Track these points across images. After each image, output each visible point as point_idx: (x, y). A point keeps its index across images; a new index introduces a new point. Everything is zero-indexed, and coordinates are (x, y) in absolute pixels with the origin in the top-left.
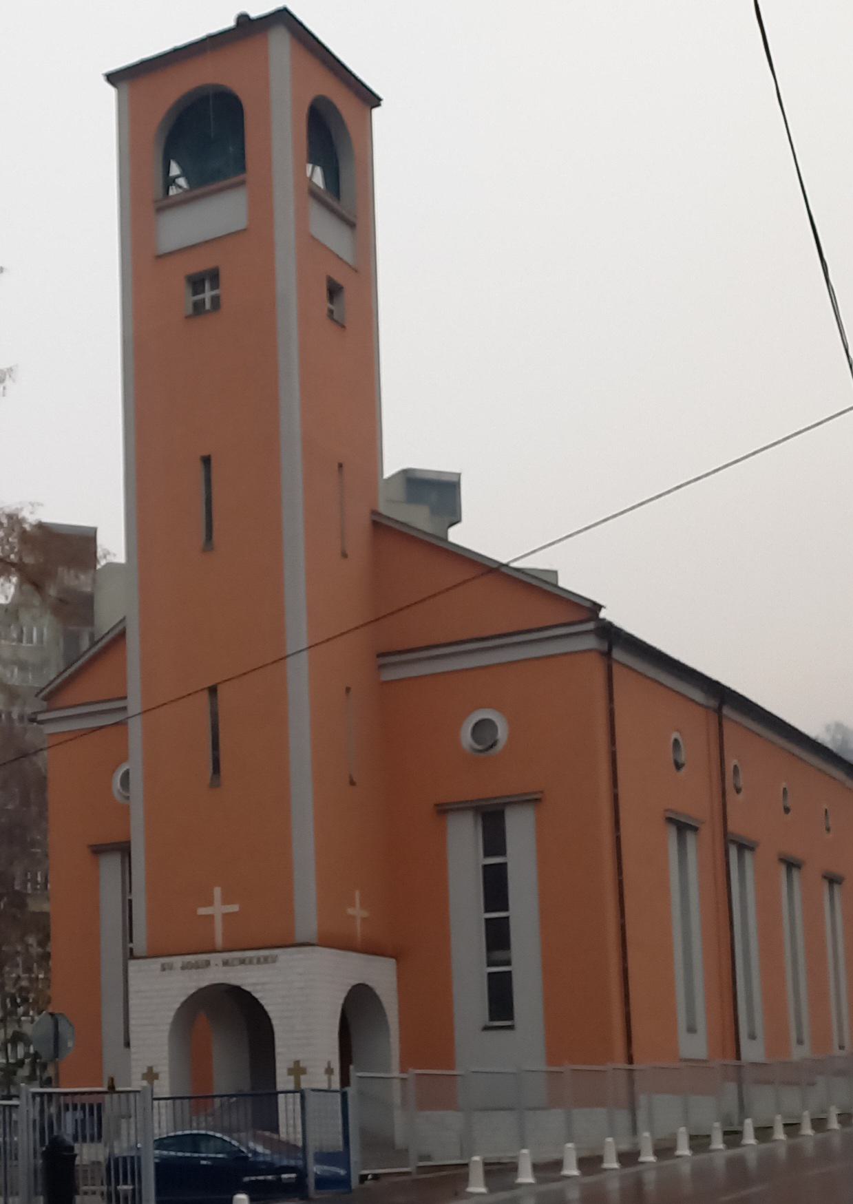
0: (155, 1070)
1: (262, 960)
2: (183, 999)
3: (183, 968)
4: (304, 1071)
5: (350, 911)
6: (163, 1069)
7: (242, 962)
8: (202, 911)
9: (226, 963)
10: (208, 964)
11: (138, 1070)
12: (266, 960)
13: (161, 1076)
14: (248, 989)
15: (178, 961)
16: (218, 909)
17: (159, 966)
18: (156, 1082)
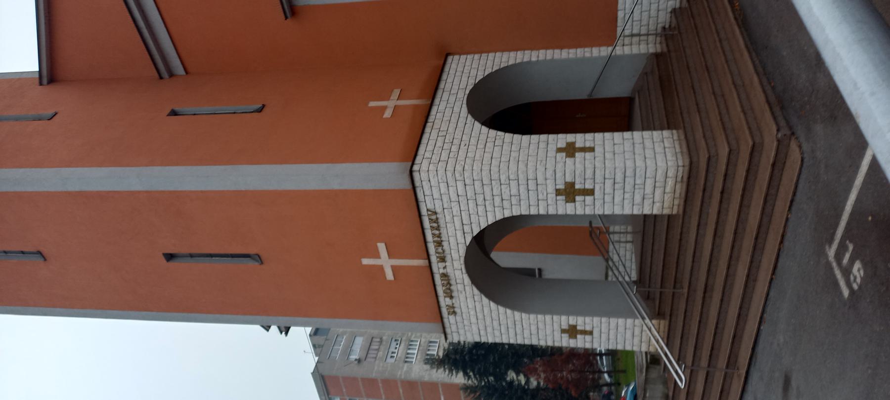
0: (565, 326)
1: (435, 225)
2: (485, 300)
3: (451, 297)
5: (388, 114)
6: (565, 321)
7: (439, 244)
8: (390, 276)
9: (443, 259)
10: (445, 276)
11: (566, 342)
12: (437, 221)
14: (469, 239)
15: (444, 302)
16: (386, 262)
17: (452, 317)
18: (579, 328)
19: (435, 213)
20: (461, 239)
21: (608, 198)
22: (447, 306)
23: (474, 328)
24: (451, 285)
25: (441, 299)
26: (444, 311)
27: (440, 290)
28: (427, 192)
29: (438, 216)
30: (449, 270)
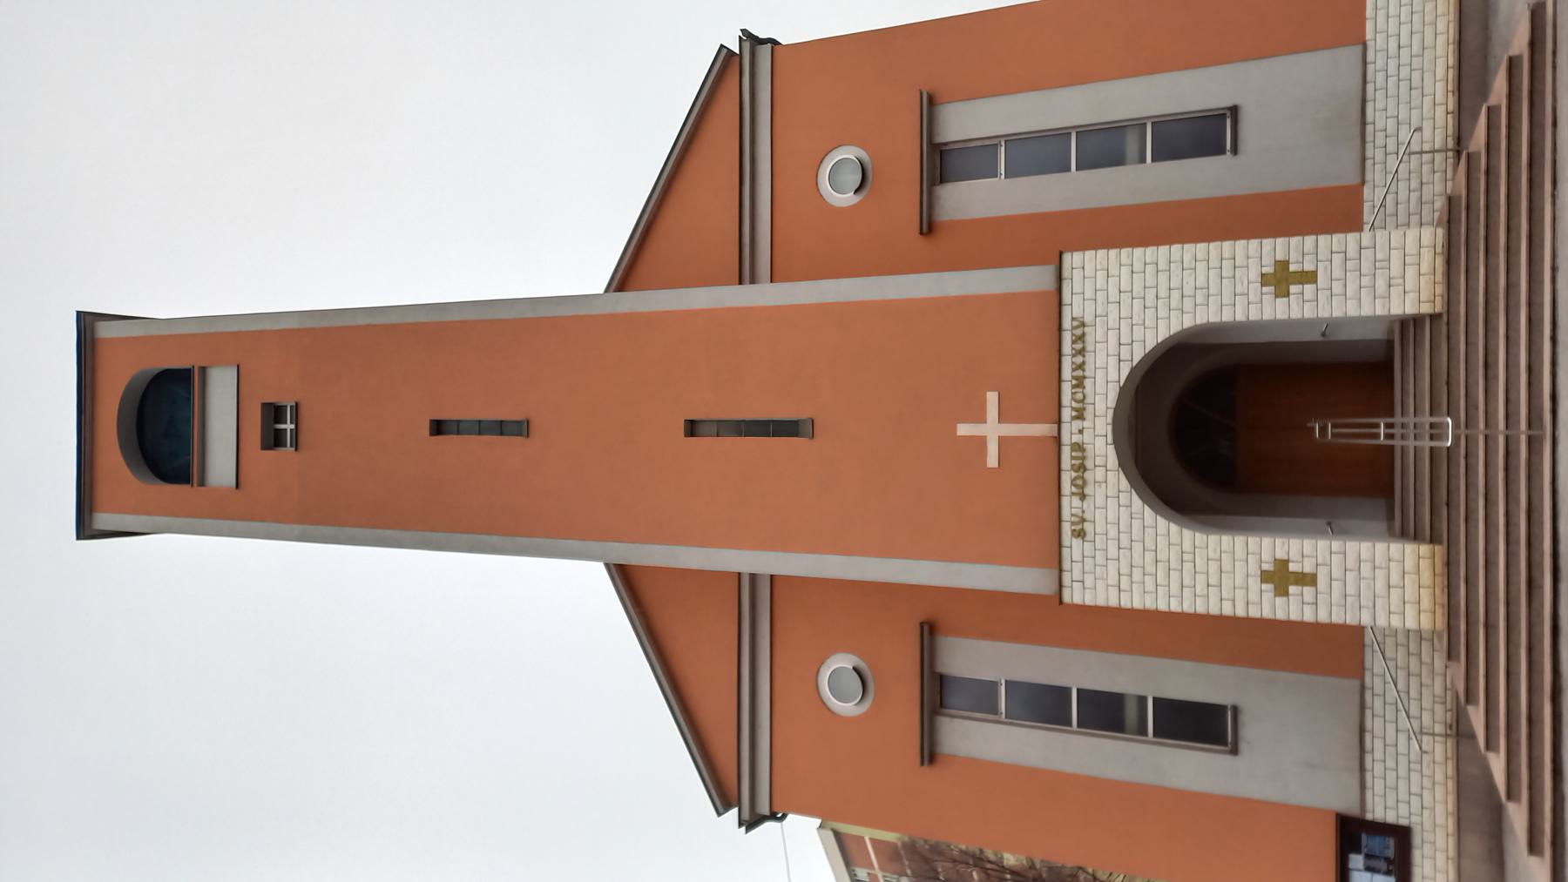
3: (1083, 497)
4: (1282, 265)
7: (1079, 383)
9: (1080, 416)
10: (1078, 447)
12: (1081, 338)
13: (1280, 555)
15: (1070, 506)
17: (1076, 543)
18: (1292, 567)
19: (1083, 325)
20: (1113, 375)
21: (1337, 288)
22: (1072, 515)
23: (1112, 566)
24: (1085, 469)
25: (1065, 502)
26: (1067, 528)
27: (1067, 487)
28: (1077, 289)
29: (1086, 329)
30: (1087, 437)
